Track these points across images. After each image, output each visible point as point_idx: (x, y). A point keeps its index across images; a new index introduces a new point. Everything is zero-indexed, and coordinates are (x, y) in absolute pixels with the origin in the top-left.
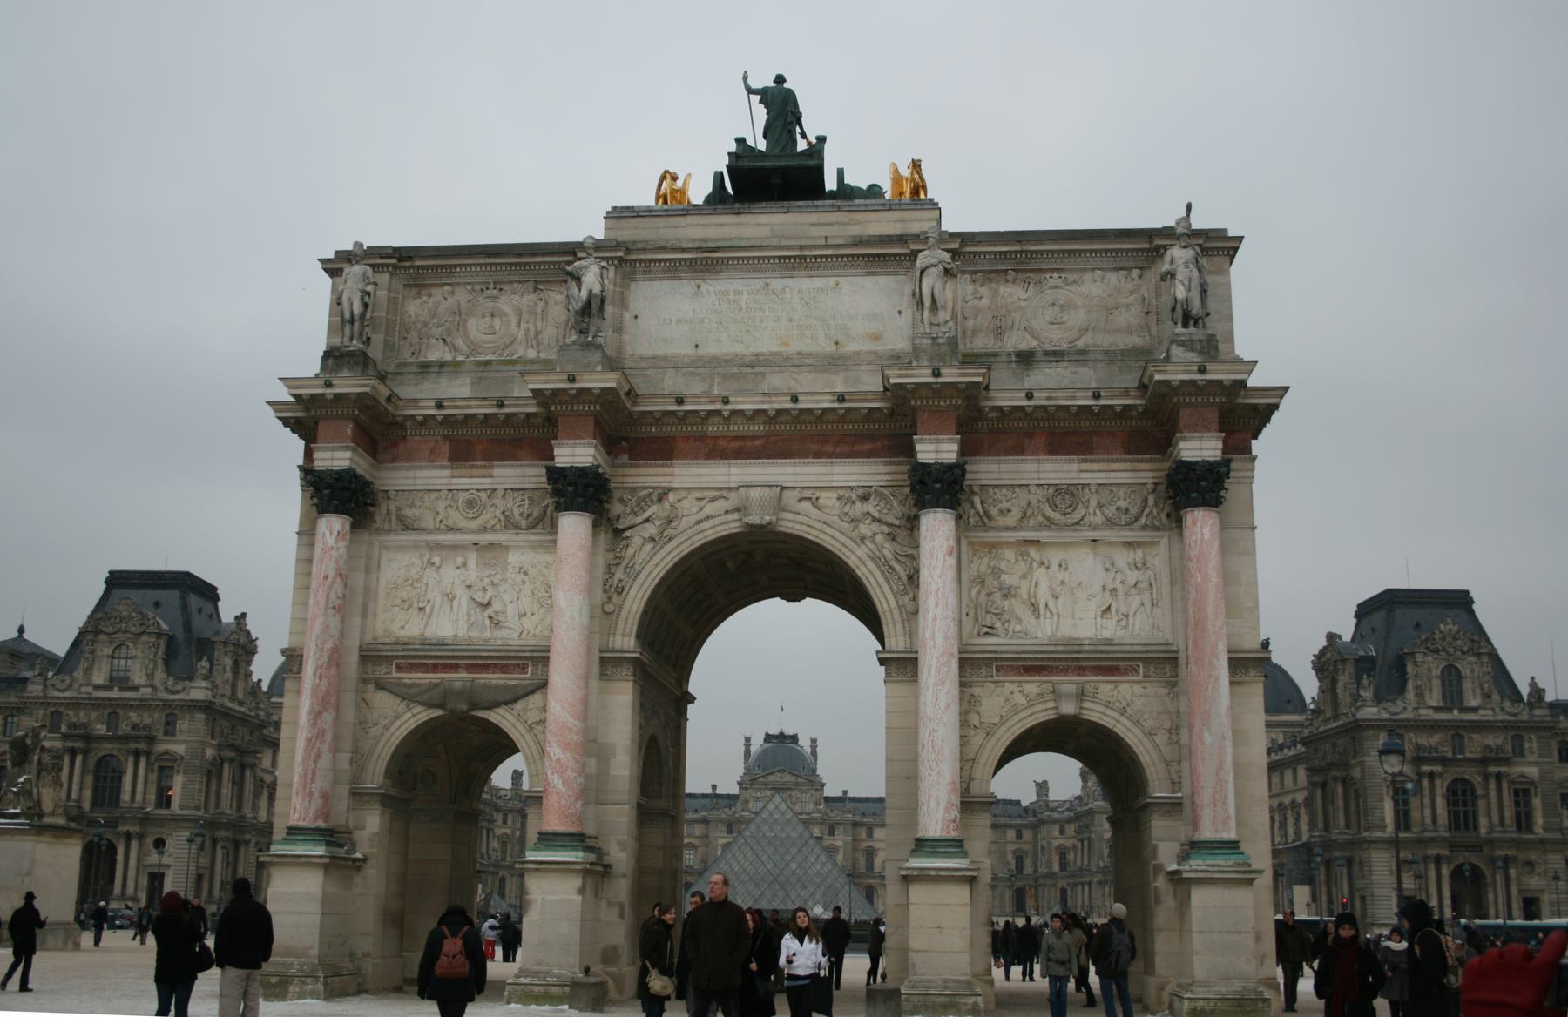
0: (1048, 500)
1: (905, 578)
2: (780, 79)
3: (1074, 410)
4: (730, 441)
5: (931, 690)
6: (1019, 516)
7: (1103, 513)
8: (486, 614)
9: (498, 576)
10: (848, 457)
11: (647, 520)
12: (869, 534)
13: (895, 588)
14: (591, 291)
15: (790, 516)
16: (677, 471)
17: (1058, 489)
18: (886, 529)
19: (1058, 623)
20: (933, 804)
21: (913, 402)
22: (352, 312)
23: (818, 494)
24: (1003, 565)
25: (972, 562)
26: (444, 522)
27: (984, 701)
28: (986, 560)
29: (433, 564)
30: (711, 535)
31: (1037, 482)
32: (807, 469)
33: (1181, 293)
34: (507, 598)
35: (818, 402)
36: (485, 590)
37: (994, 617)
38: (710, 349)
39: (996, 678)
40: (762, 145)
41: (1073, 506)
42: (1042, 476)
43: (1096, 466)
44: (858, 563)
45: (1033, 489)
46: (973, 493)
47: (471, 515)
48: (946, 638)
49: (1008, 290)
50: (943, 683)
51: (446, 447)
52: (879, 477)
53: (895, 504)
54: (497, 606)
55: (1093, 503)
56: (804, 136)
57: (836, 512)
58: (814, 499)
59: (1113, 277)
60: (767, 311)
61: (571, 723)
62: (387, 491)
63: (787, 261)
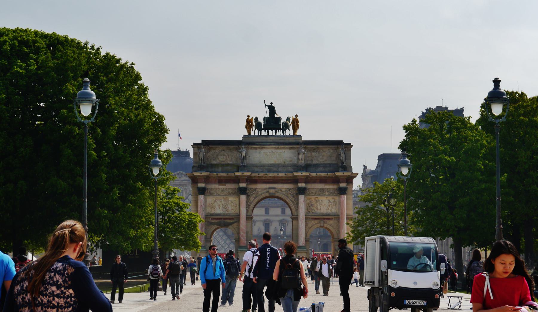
1: (296, 204)
2: (272, 103)
8: (226, 210)
11: (253, 194)
17: (321, 189)
18: (293, 196)
20: (301, 241)
22: (202, 159)
24: (312, 201)
29: (216, 201)
33: (341, 159)
34: (229, 206)
36: (225, 205)
38: (263, 163)
40: (269, 117)
41: (323, 192)
43: (327, 185)
45: (317, 189)
48: (303, 215)
49: (314, 153)
54: (228, 208)
56: (276, 113)
62: (207, 188)
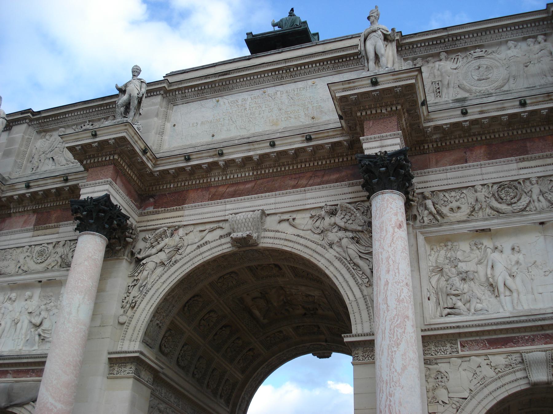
0: (493, 195)
3: (505, 118)
4: (228, 187)
5: (385, 353)
6: (468, 211)
7: (546, 199)
9: (52, 304)
10: (319, 184)
11: (161, 250)
12: (337, 239)
13: (359, 280)
14: (130, 95)
15: (271, 234)
16: (186, 212)
17: (501, 186)
18: (350, 235)
19: (518, 299)
21: (359, 114)
23: (294, 216)
24: (459, 255)
25: (430, 255)
26: (22, 267)
27: (451, 376)
28: (443, 252)
29: (11, 299)
30: (208, 256)
31: (482, 182)
32: (285, 198)
35: (290, 144)
37: (454, 298)
39: (461, 353)
42: (485, 177)
44: (327, 264)
46: (425, 198)
47: (39, 261)
48: (399, 301)
50: (398, 345)
51: (33, 218)
52: (344, 197)
53: (358, 215)
54: (45, 326)
55: (536, 190)
57: (310, 227)
58: (291, 220)
59: (523, 45)
60: (264, 106)
61: (52, 404)
63: (277, 73)
